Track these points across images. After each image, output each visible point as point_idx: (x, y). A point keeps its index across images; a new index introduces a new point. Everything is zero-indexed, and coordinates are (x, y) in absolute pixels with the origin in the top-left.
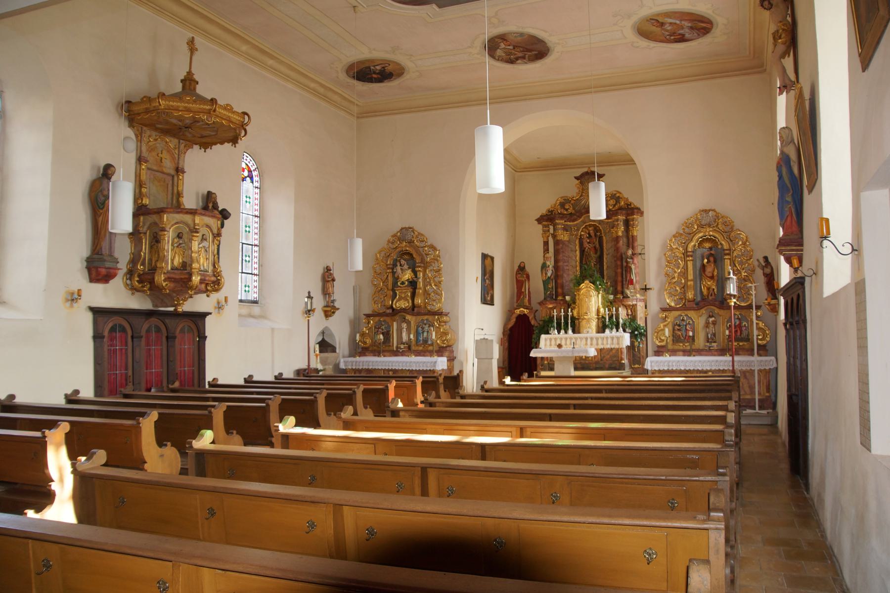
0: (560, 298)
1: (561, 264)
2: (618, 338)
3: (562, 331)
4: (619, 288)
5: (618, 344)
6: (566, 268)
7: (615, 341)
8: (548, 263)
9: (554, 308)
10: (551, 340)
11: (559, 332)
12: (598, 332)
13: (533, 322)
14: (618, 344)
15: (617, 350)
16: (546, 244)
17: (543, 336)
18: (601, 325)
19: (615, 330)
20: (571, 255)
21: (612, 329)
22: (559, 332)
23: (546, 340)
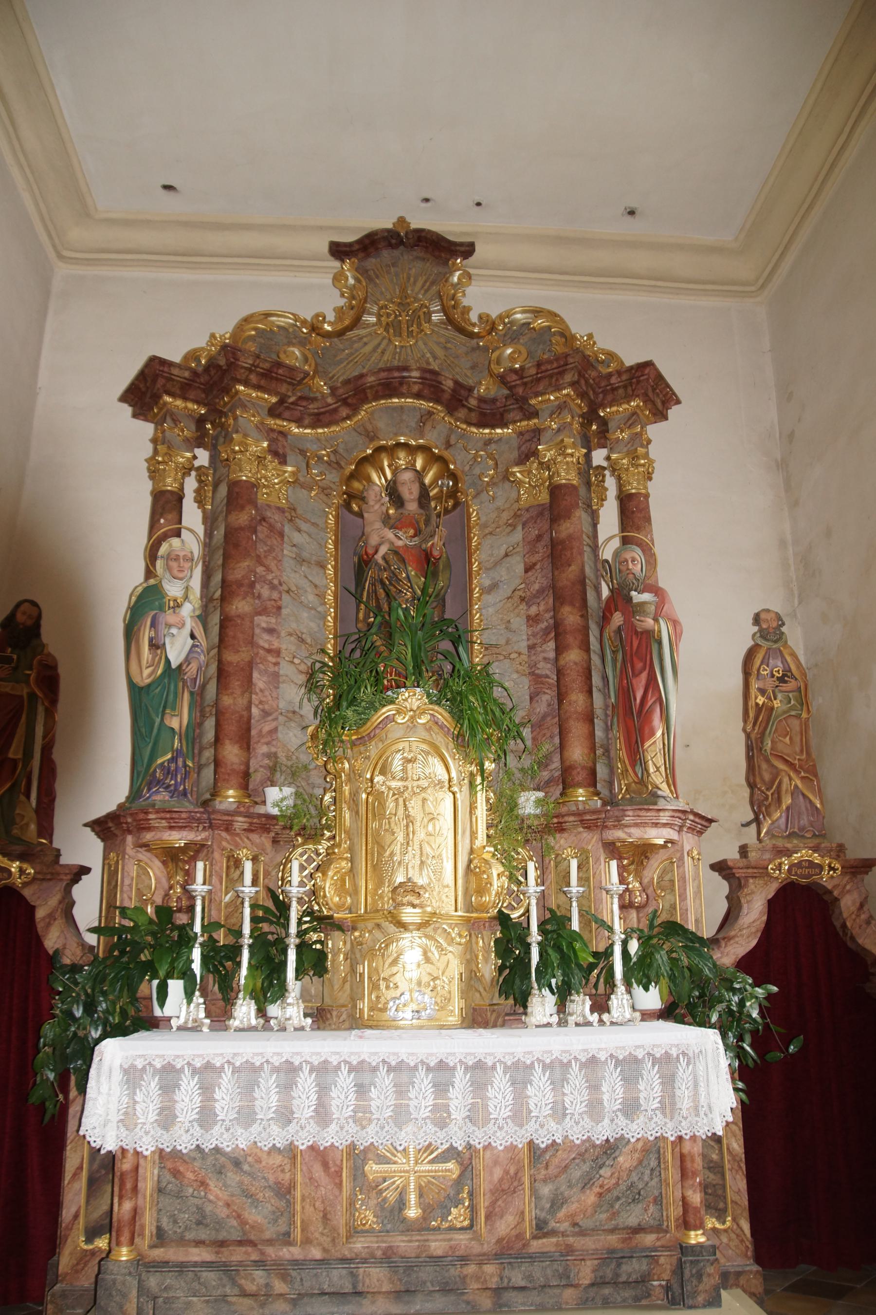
0: (231, 796)
1: (240, 606)
2: (666, 1064)
3: (245, 1010)
4: (577, 753)
5: (668, 1106)
6: (264, 640)
7: (650, 1089)
8: (173, 589)
9: (196, 850)
10: (169, 1077)
11: (220, 1015)
12: (476, 1019)
13: (52, 941)
14: (668, 1106)
15: (653, 1149)
16: (166, 504)
17: (113, 1054)
18: (488, 967)
19: (581, 1004)
20: (292, 576)
21: (563, 994)
22: (220, 1015)
23: (132, 1076)
